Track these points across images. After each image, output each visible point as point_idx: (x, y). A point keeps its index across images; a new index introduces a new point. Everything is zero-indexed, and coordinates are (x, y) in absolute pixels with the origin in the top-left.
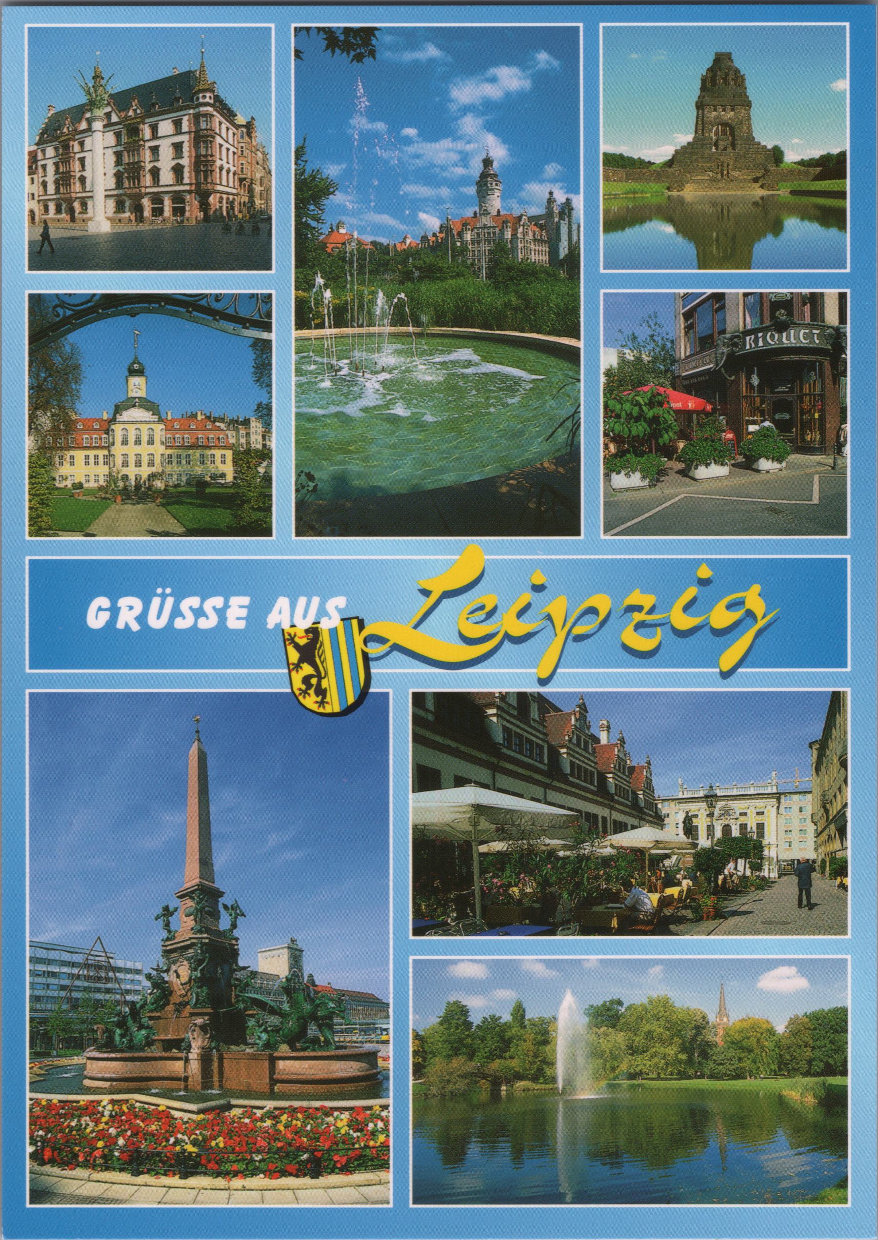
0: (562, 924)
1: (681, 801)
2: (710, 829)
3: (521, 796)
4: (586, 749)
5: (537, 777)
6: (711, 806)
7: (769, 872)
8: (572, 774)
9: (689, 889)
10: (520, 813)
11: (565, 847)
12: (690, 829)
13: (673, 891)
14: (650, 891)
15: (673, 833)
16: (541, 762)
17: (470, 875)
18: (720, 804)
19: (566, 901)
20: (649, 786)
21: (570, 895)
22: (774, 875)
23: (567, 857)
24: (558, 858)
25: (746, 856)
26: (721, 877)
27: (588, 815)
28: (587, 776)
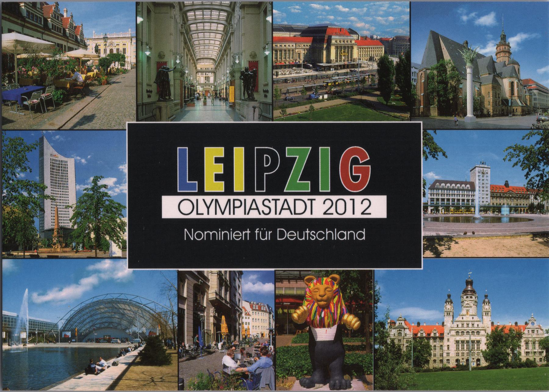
0: (48, 86)
1: (95, 39)
2: (105, 51)
3: (33, 37)
4: (58, 19)
5: (39, 29)
6: (106, 41)
7: (128, 67)
8: (53, 29)
9: (97, 73)
10: (33, 43)
11: (50, 57)
12: (97, 50)
13: (91, 74)
14: (82, 73)
15: (91, 51)
16: (41, 24)
17: (14, 66)
18: (109, 41)
19: (50, 78)
20: (82, 34)
21: (52, 74)
22: (129, 68)
23: (50, 60)
24: (47, 61)
25: (119, 61)
26: (109, 69)
27: (58, 45)
28: (59, 30)
